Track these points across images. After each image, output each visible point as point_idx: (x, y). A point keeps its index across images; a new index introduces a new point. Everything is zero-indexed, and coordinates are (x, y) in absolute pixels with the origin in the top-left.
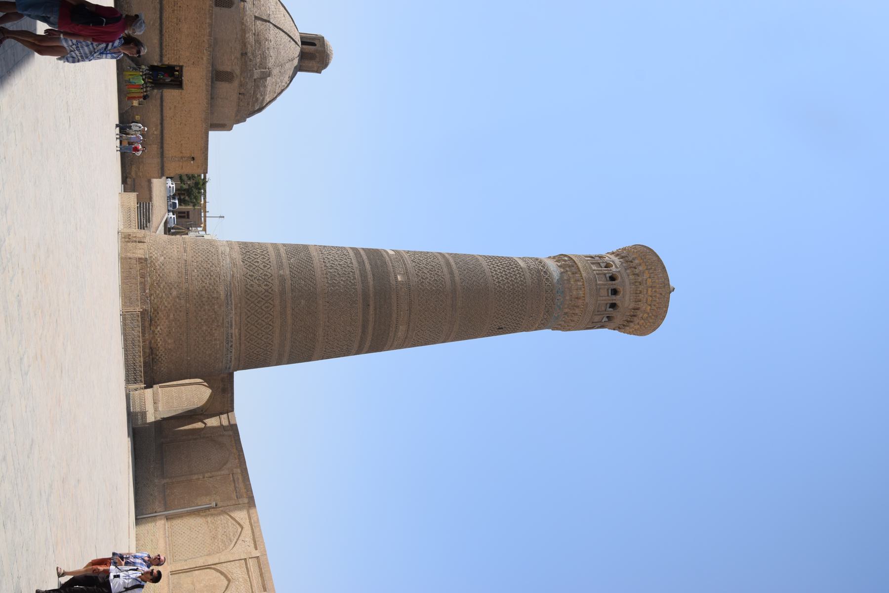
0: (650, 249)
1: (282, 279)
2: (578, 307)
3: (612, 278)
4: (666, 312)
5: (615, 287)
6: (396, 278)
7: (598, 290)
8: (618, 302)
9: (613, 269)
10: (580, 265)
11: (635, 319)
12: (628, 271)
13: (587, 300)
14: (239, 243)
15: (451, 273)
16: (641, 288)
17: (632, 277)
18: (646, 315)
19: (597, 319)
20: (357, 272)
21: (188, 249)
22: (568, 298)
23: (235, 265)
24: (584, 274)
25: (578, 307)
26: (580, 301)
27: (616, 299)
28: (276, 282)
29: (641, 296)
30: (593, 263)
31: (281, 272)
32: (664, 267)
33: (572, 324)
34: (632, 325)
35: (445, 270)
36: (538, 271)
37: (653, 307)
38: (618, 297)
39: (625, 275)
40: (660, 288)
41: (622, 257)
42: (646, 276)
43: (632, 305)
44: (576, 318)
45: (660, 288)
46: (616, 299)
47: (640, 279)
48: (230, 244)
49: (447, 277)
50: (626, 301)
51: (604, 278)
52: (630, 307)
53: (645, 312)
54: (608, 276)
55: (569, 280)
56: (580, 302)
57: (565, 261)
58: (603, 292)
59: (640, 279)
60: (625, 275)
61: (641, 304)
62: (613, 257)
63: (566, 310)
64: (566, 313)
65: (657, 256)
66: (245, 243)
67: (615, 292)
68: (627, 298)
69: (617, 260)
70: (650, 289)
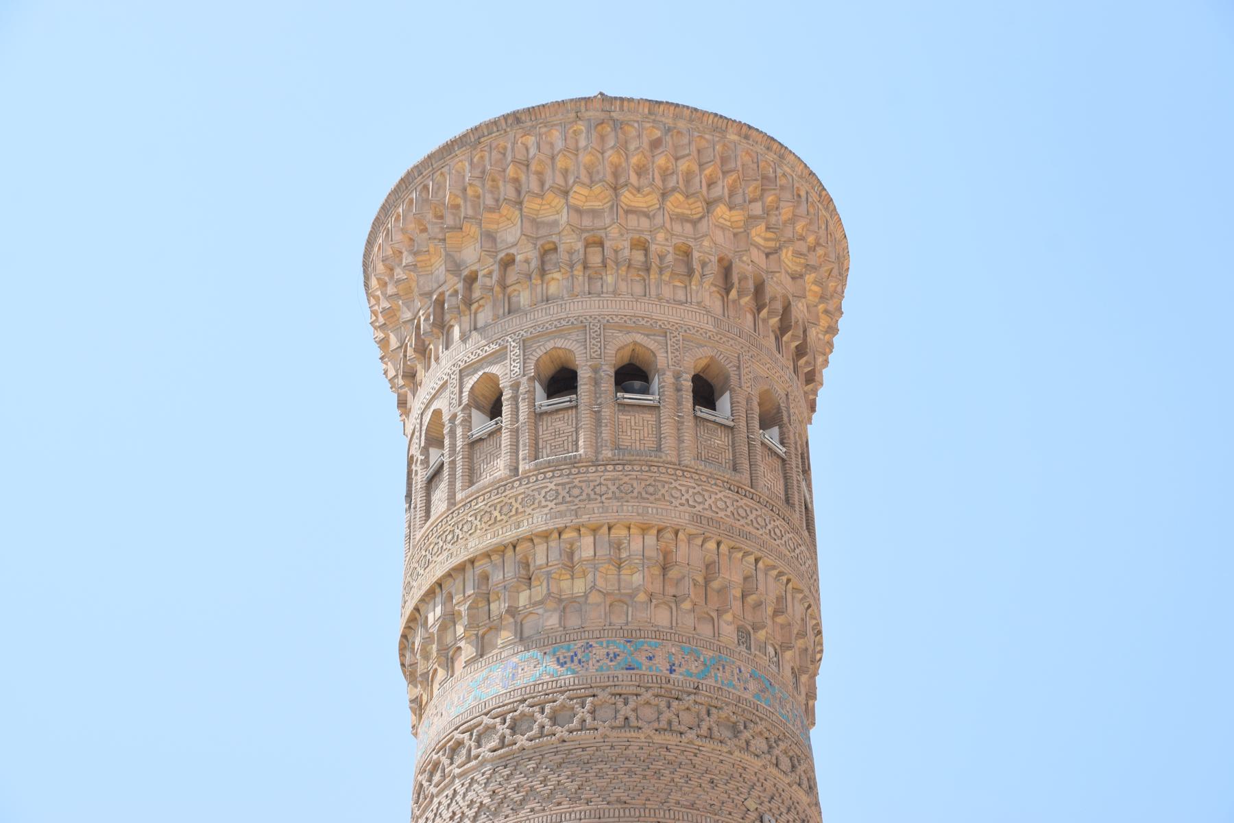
0: (406, 182)
2: (710, 569)
3: (561, 381)
4: (746, 131)
5: (608, 373)
7: (624, 458)
8: (691, 363)
9: (506, 372)
10: (477, 543)
11: (771, 289)
12: (524, 298)
13: (678, 516)
16: (617, 240)
17: (556, 283)
18: (758, 234)
19: (770, 480)
22: (662, 617)
24: (537, 521)
25: (710, 569)
26: (682, 552)
27: (672, 372)
29: (660, 243)
30: (471, 476)
32: (515, 118)
33: (796, 609)
34: (799, 310)
36: (509, 760)
37: (719, 190)
38: (662, 360)
39: (542, 317)
40: (623, 146)
41: (442, 327)
42: (555, 211)
43: (706, 292)
44: (769, 589)
45: (623, 146)
46: (672, 372)
47: (571, 242)
50: (684, 327)
51: (561, 424)
52: (717, 306)
53: (740, 235)
54: (542, 402)
55: (564, 604)
56: (688, 555)
57: (450, 619)
58: (636, 429)
59: (571, 242)
60: (542, 317)
61: (706, 251)
62: (429, 380)
63: (728, 631)
64: (744, 636)
65: (448, 149)
69: (451, 358)
70: (627, 197)
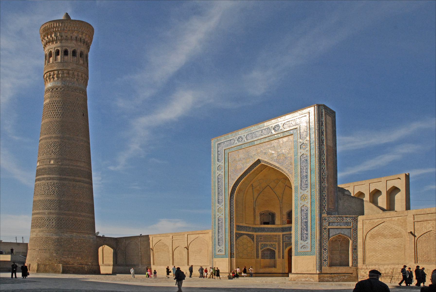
2: (73, 73)
6: (52, 164)
14: (32, 228)
15: (51, 138)
21: (34, 248)
23: (42, 231)
24: (55, 68)
25: (73, 73)
26: (70, 72)
27: (70, 51)
35: (48, 140)
48: (32, 232)
49: (53, 140)
52: (75, 43)
61: (74, 37)
63: (75, 80)
64: (77, 80)
66: (32, 226)
67: (66, 53)
68: (70, 45)
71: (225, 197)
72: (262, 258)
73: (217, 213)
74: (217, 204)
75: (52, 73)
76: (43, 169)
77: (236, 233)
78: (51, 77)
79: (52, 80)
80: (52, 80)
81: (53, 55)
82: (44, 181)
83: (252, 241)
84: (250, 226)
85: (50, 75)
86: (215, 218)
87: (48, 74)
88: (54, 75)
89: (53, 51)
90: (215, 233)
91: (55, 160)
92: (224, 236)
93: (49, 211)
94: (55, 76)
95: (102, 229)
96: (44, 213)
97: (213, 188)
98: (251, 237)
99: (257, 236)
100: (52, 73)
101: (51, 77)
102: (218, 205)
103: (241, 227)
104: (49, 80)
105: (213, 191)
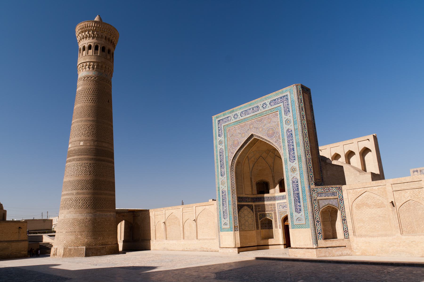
1: (78, 194)
20: (78, 162)
24: (87, 60)
28: (78, 196)
31: (75, 194)
71: (227, 169)
72: (262, 229)
73: (221, 186)
74: (220, 177)
75: (85, 64)
76: (74, 150)
77: (238, 205)
78: (84, 67)
79: (84, 70)
80: (84, 70)
81: (86, 49)
82: (74, 162)
83: (251, 212)
84: (249, 196)
85: (83, 66)
86: (219, 190)
87: (81, 65)
88: (86, 65)
89: (86, 46)
90: (220, 206)
91: (85, 141)
92: (228, 208)
93: (77, 191)
94: (87, 66)
95: (121, 204)
96: (73, 194)
97: (216, 161)
98: (250, 207)
99: (255, 206)
100: (85, 64)
101: (84, 67)
102: (221, 177)
103: (242, 198)
104: (82, 70)
105: (216, 164)
